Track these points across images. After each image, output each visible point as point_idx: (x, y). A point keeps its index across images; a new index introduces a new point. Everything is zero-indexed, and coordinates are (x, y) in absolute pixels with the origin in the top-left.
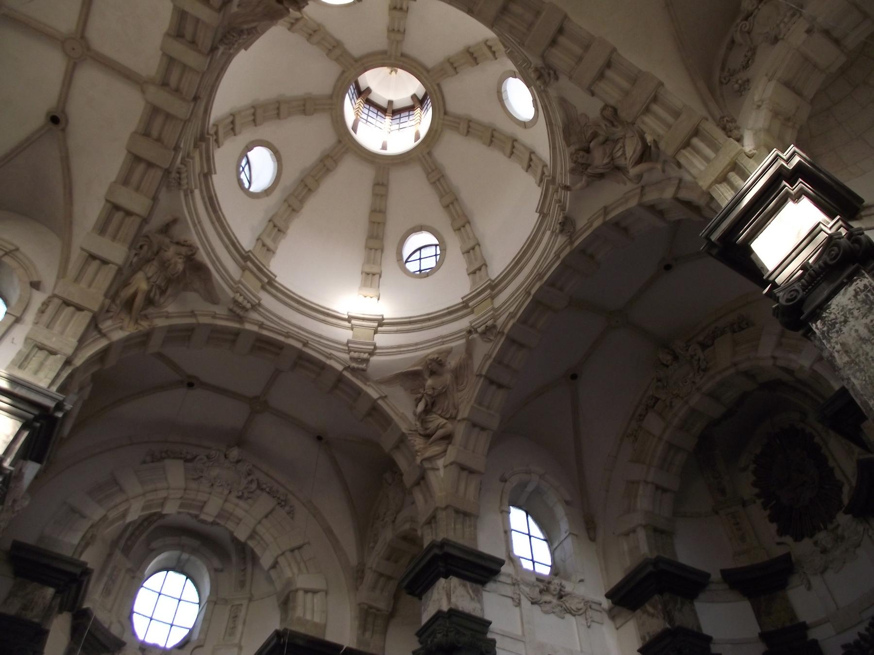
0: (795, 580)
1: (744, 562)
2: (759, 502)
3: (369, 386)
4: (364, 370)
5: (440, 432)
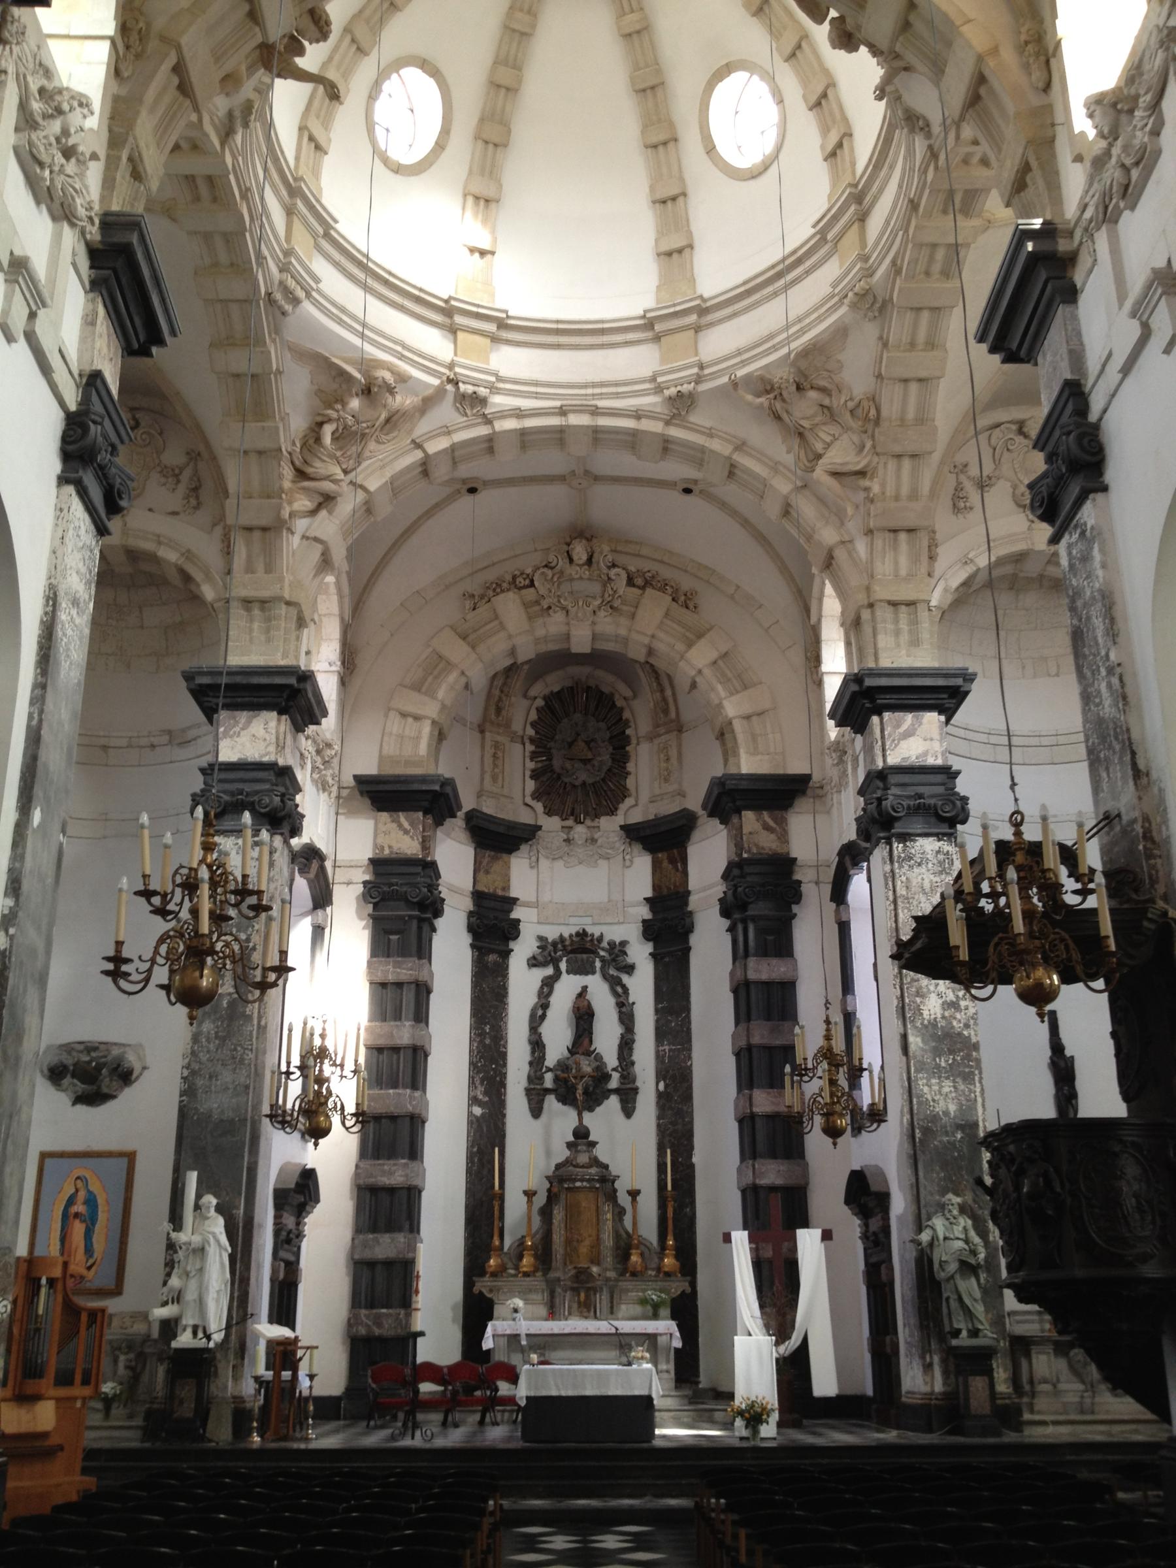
0: (524, 848)
1: (489, 808)
2: (530, 748)
3: (274, 341)
4: (284, 314)
5: (327, 486)
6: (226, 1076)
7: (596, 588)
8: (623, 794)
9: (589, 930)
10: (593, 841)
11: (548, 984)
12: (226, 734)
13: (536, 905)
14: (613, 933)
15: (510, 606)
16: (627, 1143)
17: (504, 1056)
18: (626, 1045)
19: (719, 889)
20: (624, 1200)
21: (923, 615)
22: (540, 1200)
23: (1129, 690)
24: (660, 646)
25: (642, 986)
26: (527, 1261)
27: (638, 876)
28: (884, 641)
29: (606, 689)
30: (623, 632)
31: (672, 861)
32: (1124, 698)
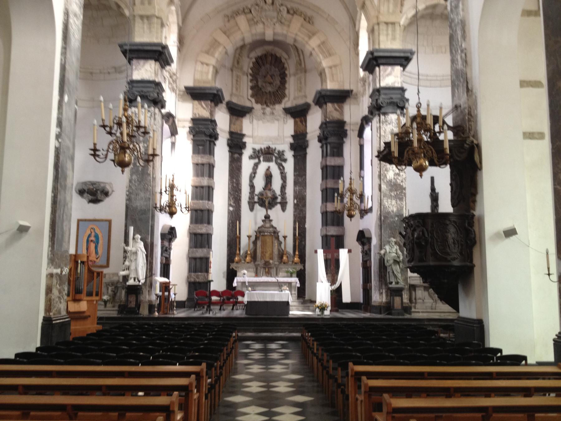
0: (248, 116)
1: (235, 100)
2: (250, 77)
6: (142, 195)
7: (275, 14)
8: (284, 96)
9: (271, 146)
10: (273, 113)
11: (256, 166)
12: (136, 69)
13: (252, 137)
14: (280, 147)
15: (242, 21)
16: (283, 220)
17: (240, 190)
18: (283, 187)
19: (318, 132)
20: (281, 239)
21: (397, 28)
22: (253, 239)
23: (468, 59)
24: (299, 39)
25: (289, 166)
26: (248, 259)
27: (289, 127)
28: (382, 38)
29: (278, 55)
30: (285, 32)
31: (301, 122)
32: (466, 62)
